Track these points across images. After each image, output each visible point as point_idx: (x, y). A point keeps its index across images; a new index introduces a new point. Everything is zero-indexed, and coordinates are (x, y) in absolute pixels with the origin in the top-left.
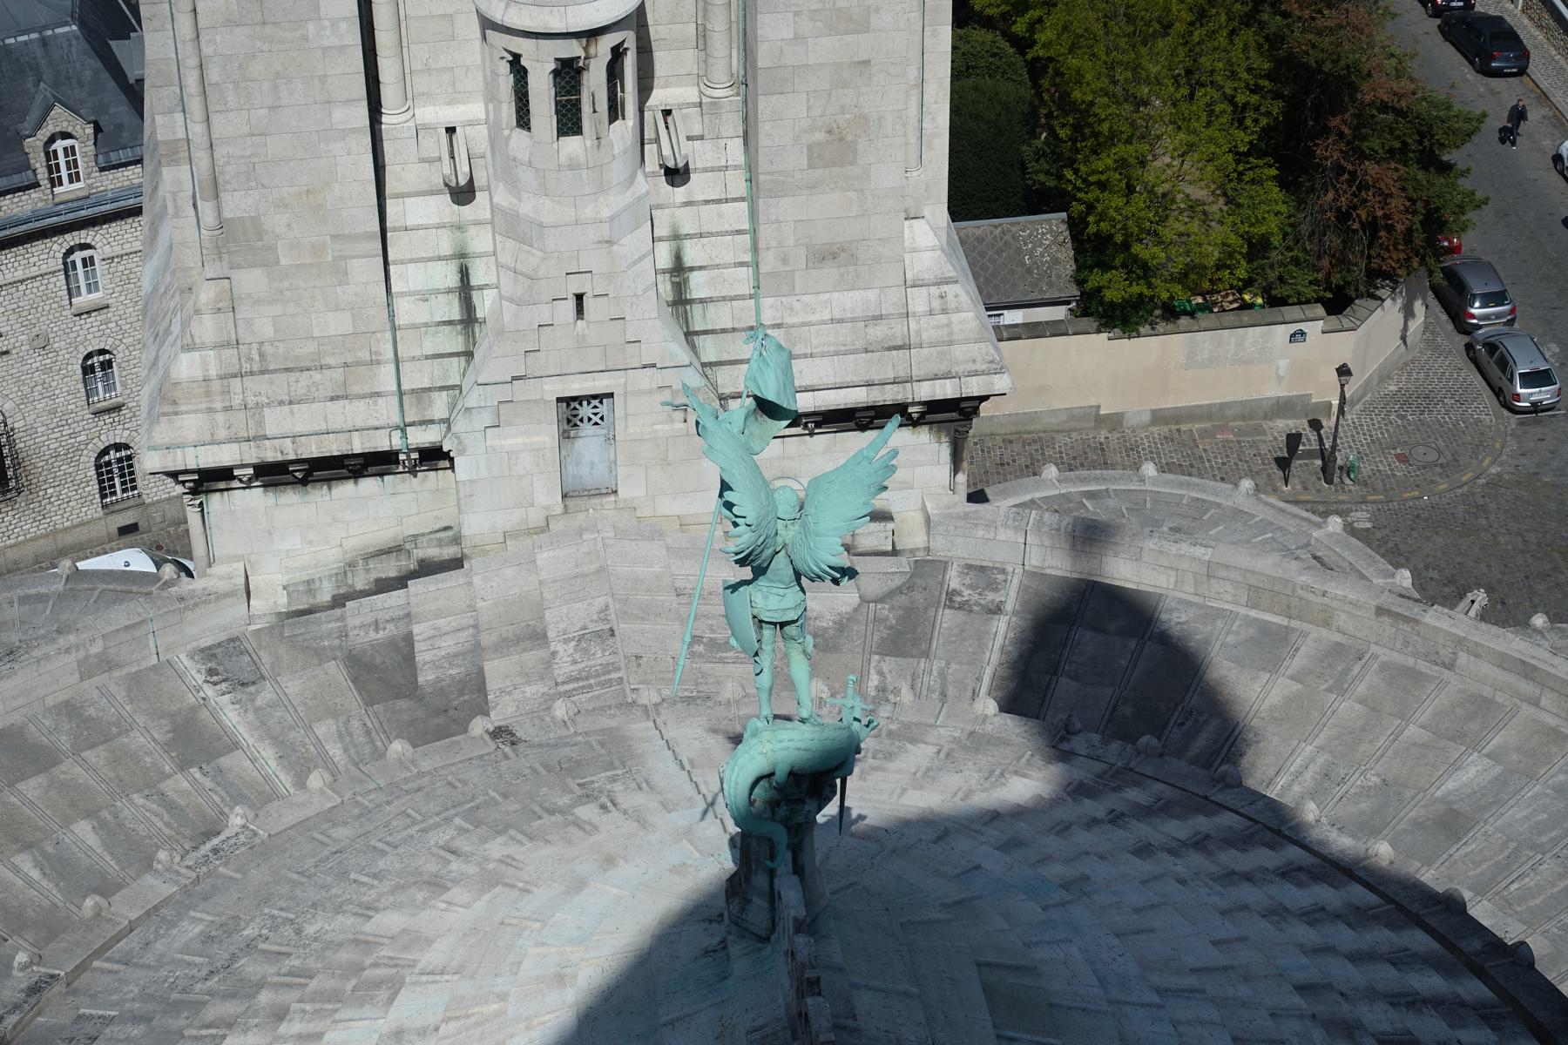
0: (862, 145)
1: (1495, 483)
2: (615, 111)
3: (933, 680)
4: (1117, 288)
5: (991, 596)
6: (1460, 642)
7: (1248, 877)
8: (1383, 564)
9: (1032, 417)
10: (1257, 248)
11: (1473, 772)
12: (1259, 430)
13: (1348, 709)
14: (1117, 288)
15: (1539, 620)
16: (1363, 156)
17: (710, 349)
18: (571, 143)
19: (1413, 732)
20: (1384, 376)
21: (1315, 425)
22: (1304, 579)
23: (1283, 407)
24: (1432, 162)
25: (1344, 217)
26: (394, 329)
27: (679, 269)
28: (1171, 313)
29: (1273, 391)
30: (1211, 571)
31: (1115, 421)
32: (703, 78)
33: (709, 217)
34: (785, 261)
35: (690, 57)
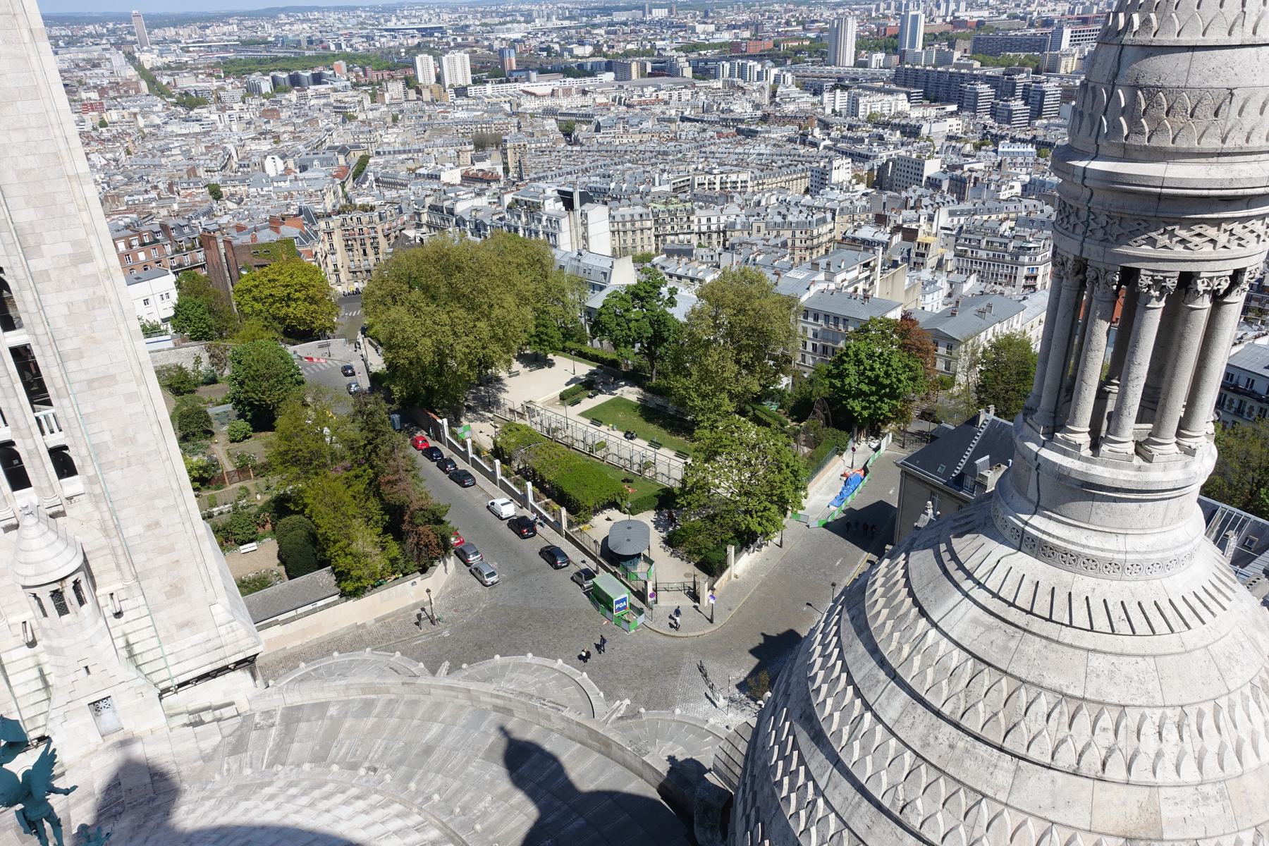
0: (184, 587)
1: (485, 610)
2: (81, 602)
3: (248, 760)
4: (350, 586)
5: (270, 721)
6: (429, 686)
7: (328, 811)
8: (414, 662)
9: (336, 632)
10: (393, 561)
11: (436, 729)
12: (410, 615)
13: (394, 721)
14: (350, 586)
15: (464, 666)
16: (417, 526)
17: (146, 669)
18: (65, 617)
19: (415, 722)
20: (446, 587)
21: (423, 609)
22: (378, 681)
23: (415, 606)
24: (442, 522)
25: (417, 544)
26: (15, 699)
27: (128, 645)
28: (374, 587)
29: (412, 602)
30: (347, 687)
31: (363, 626)
32: (123, 579)
33: (136, 625)
34: (168, 632)
35: (116, 574)
